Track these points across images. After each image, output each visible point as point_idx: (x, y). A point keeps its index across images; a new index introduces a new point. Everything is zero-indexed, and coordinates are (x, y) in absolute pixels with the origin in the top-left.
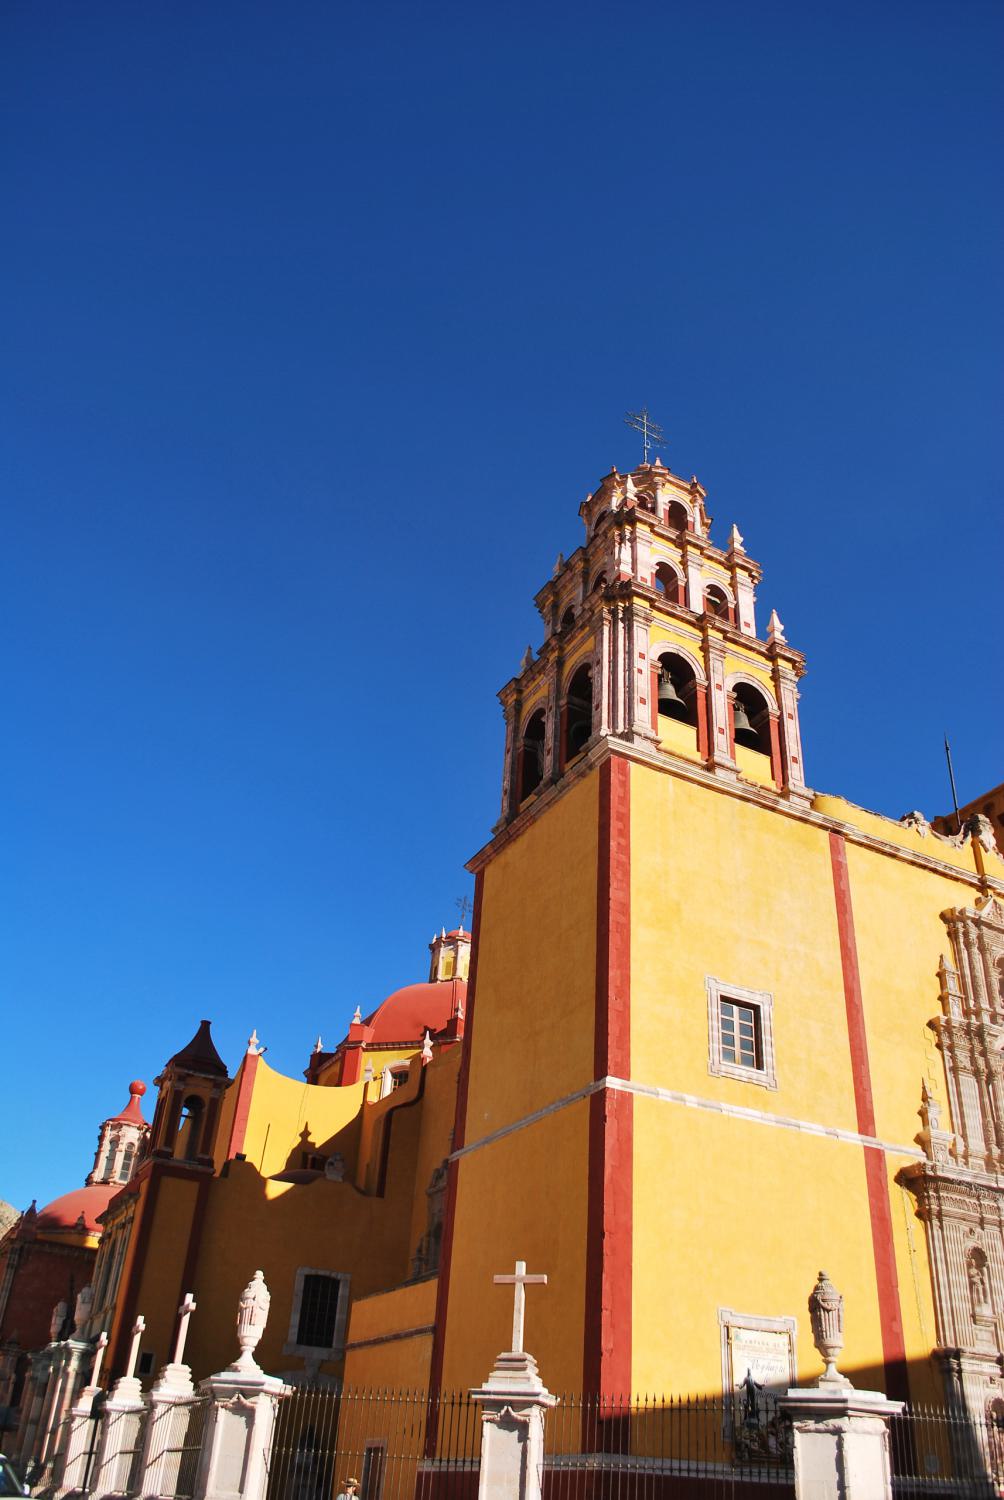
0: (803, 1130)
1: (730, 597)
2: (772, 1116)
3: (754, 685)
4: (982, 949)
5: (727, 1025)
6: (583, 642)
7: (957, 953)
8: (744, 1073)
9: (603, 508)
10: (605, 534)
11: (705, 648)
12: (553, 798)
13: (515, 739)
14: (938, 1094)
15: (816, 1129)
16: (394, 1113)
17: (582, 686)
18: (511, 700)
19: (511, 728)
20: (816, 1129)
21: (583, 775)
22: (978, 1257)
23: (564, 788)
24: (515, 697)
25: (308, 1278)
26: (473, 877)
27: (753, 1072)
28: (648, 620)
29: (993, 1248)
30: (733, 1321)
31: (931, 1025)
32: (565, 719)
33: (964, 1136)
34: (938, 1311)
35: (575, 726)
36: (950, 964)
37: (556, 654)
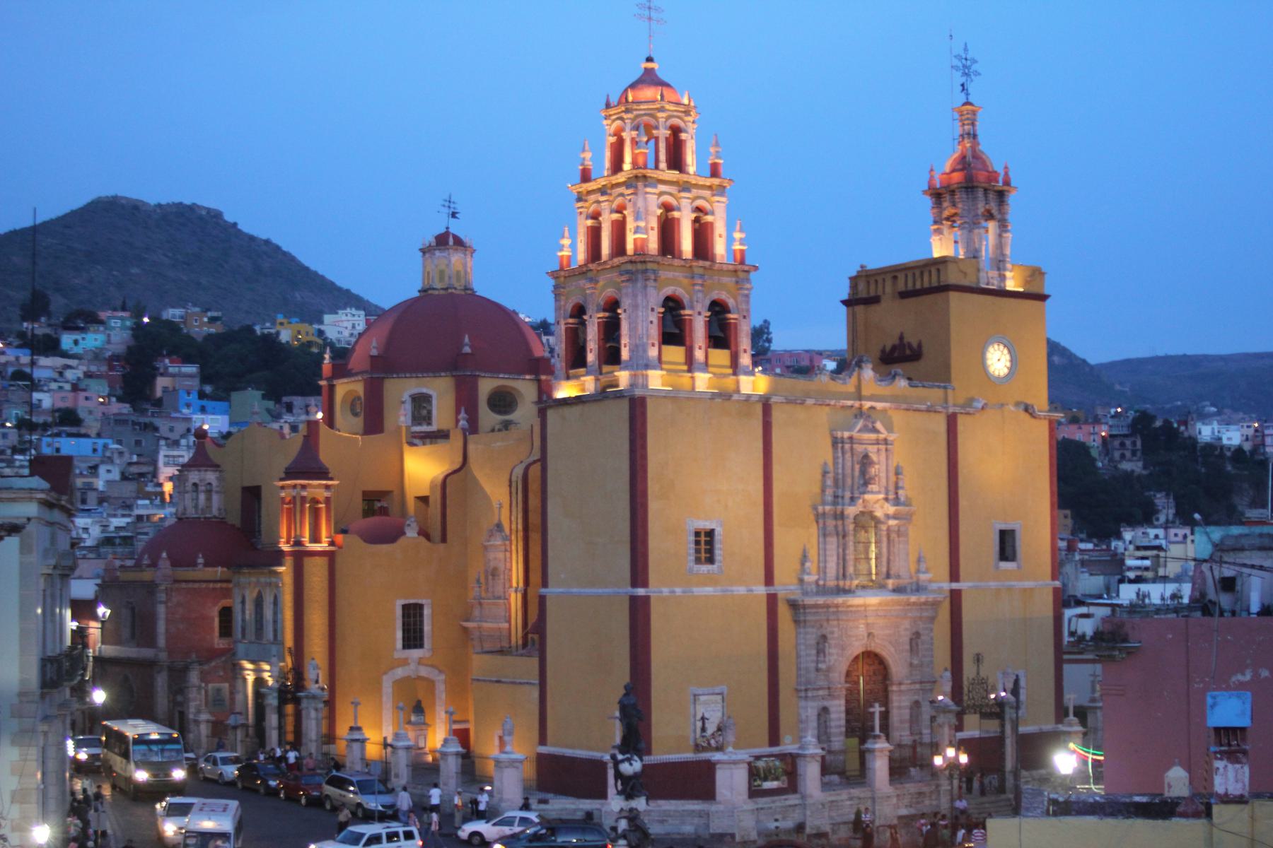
2: (719, 588)
4: (852, 455)
5: (697, 543)
7: (835, 458)
14: (813, 553)
20: (741, 590)
21: (619, 397)
25: (405, 607)
27: (710, 567)
29: (832, 633)
30: (697, 693)
31: (815, 508)
33: (825, 573)
34: (799, 669)
35: (608, 345)
36: (830, 467)
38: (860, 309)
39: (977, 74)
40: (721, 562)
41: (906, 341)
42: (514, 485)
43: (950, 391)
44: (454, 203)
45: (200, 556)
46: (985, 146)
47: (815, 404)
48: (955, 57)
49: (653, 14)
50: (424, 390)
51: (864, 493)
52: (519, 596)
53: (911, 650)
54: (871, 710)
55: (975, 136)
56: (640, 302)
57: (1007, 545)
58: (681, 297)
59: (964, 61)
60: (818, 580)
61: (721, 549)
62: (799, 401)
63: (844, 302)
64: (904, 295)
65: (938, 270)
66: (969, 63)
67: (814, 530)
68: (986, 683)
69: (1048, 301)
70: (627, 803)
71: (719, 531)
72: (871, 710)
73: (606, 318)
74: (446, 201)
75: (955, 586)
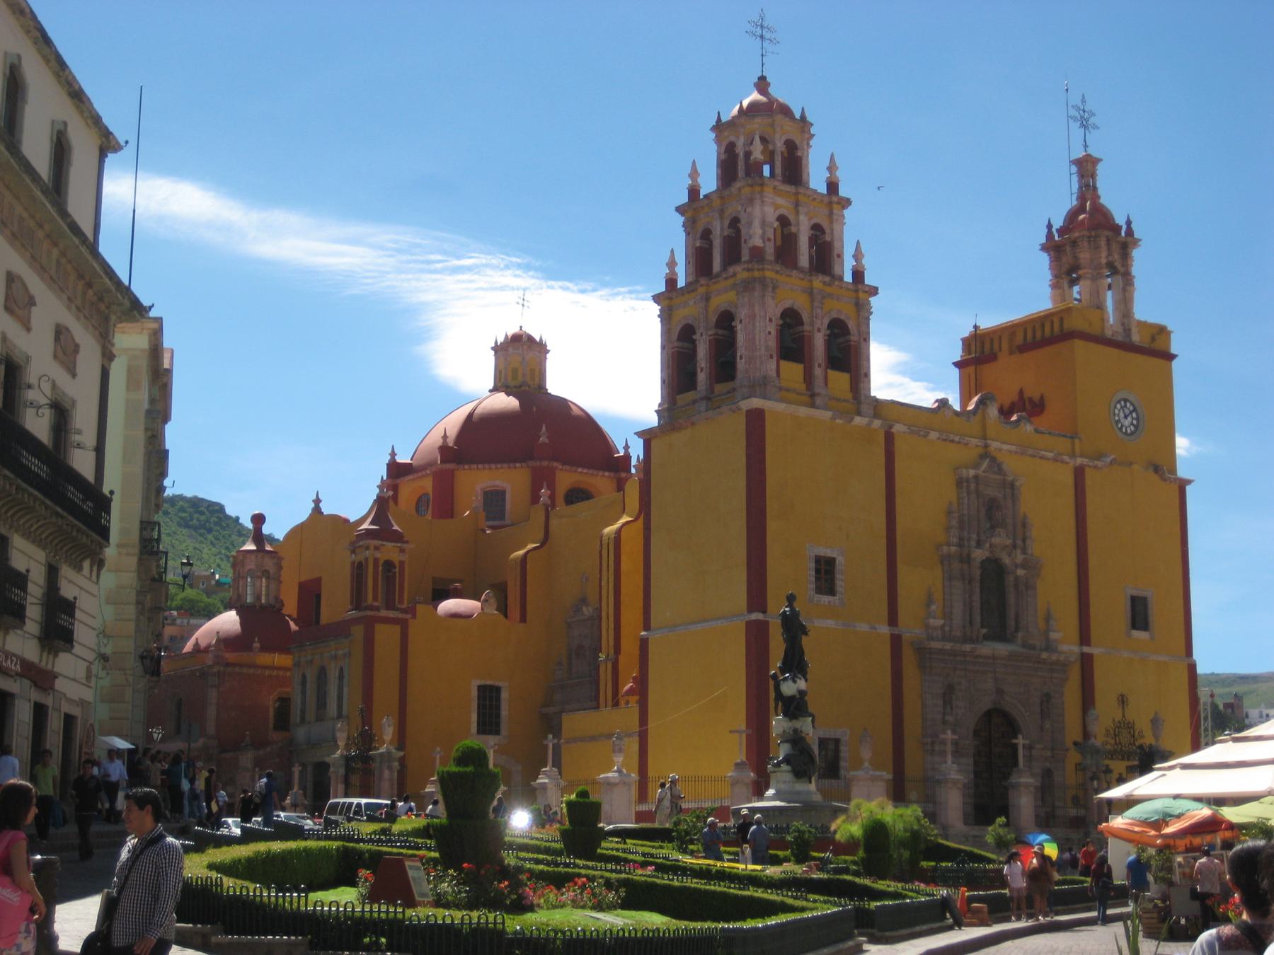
1: (827, 231)
3: (842, 317)
5: (818, 571)
8: (826, 600)
9: (732, 138)
10: (740, 189)
11: (812, 301)
15: (863, 627)
17: (726, 320)
20: (863, 627)
22: (950, 689)
25: (479, 687)
26: (641, 441)
28: (775, 288)
35: (722, 360)
38: (971, 369)
39: (1096, 127)
40: (842, 594)
41: (1026, 396)
42: (605, 547)
43: (1077, 441)
44: (527, 301)
45: (256, 639)
46: (1108, 198)
47: (938, 439)
48: (1072, 106)
49: (767, 35)
51: (992, 536)
52: (610, 665)
53: (1042, 710)
54: (1015, 741)
55: (1095, 188)
56: (757, 311)
57: (1139, 615)
58: (800, 311)
59: (1082, 113)
60: (944, 625)
61: (842, 580)
62: (922, 433)
63: (957, 364)
64: (1024, 348)
65: (1062, 319)
66: (1086, 115)
68: (1133, 728)
69: (1175, 363)
70: (790, 724)
71: (840, 560)
72: (1015, 741)
73: (722, 335)
74: (520, 298)
75: (1086, 649)
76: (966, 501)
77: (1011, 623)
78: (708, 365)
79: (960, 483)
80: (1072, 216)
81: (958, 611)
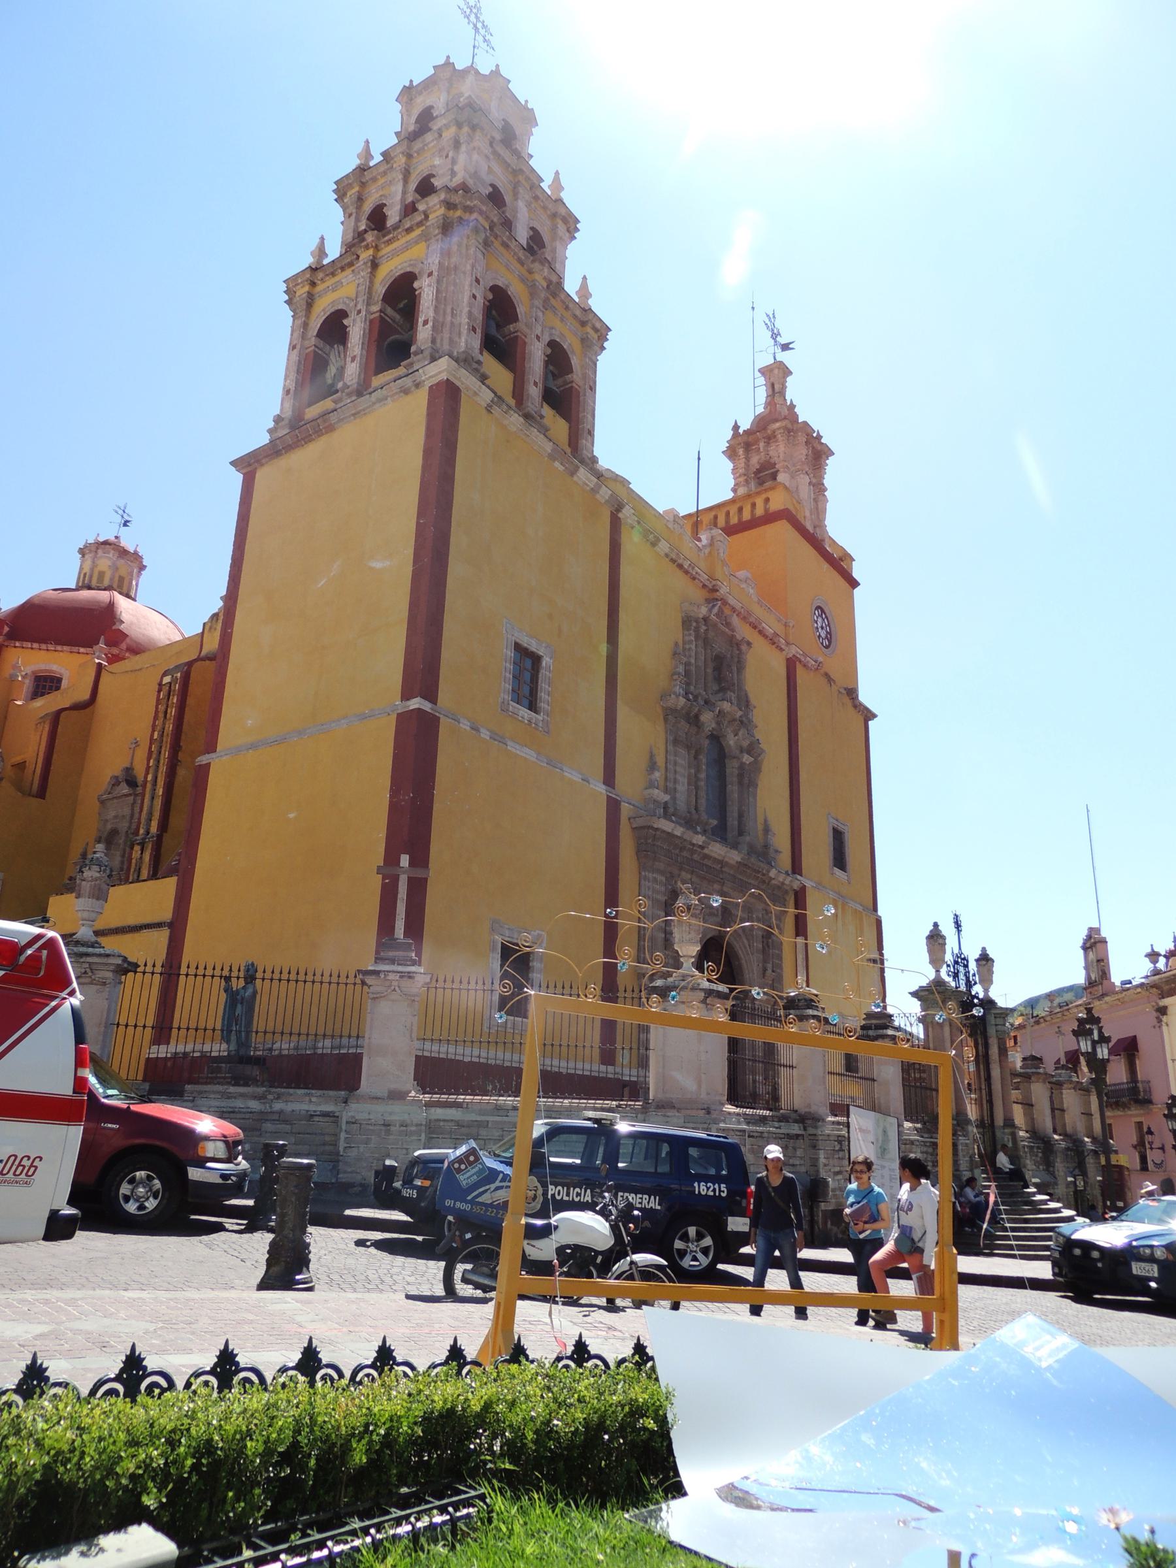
0: (566, 774)
6: (406, 248)
7: (684, 643)
9: (428, 103)
12: (364, 410)
13: (304, 336)
14: (660, 760)
16: (63, 714)
18: (303, 291)
19: (299, 322)
21: (406, 391)
23: (380, 400)
24: (307, 288)
26: (240, 477)
32: (377, 325)
37: (371, 252)
47: (667, 555)
49: (482, 31)
50: (54, 667)
65: (767, 500)
67: (660, 727)
69: (856, 591)
71: (546, 661)
76: (693, 647)
77: (732, 822)
78: (365, 352)
79: (687, 622)
80: (761, 423)
81: (682, 787)
